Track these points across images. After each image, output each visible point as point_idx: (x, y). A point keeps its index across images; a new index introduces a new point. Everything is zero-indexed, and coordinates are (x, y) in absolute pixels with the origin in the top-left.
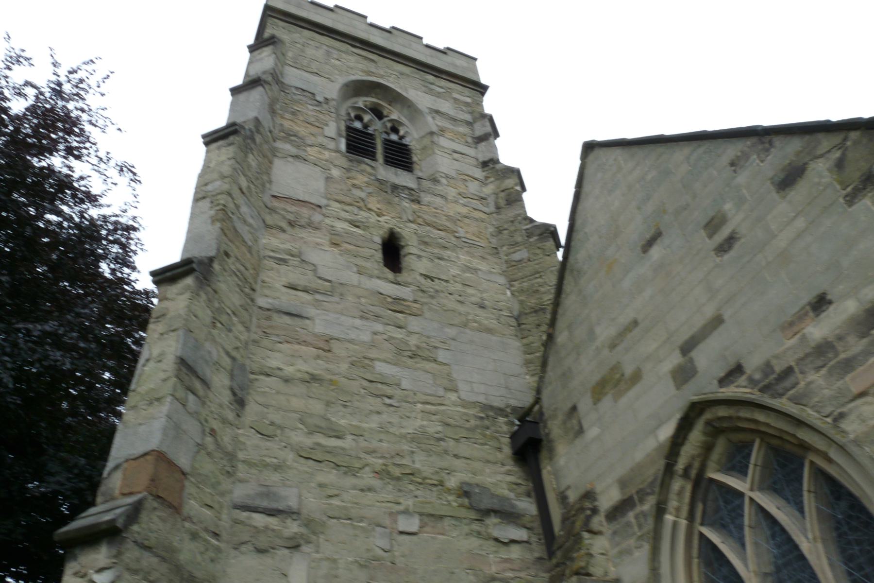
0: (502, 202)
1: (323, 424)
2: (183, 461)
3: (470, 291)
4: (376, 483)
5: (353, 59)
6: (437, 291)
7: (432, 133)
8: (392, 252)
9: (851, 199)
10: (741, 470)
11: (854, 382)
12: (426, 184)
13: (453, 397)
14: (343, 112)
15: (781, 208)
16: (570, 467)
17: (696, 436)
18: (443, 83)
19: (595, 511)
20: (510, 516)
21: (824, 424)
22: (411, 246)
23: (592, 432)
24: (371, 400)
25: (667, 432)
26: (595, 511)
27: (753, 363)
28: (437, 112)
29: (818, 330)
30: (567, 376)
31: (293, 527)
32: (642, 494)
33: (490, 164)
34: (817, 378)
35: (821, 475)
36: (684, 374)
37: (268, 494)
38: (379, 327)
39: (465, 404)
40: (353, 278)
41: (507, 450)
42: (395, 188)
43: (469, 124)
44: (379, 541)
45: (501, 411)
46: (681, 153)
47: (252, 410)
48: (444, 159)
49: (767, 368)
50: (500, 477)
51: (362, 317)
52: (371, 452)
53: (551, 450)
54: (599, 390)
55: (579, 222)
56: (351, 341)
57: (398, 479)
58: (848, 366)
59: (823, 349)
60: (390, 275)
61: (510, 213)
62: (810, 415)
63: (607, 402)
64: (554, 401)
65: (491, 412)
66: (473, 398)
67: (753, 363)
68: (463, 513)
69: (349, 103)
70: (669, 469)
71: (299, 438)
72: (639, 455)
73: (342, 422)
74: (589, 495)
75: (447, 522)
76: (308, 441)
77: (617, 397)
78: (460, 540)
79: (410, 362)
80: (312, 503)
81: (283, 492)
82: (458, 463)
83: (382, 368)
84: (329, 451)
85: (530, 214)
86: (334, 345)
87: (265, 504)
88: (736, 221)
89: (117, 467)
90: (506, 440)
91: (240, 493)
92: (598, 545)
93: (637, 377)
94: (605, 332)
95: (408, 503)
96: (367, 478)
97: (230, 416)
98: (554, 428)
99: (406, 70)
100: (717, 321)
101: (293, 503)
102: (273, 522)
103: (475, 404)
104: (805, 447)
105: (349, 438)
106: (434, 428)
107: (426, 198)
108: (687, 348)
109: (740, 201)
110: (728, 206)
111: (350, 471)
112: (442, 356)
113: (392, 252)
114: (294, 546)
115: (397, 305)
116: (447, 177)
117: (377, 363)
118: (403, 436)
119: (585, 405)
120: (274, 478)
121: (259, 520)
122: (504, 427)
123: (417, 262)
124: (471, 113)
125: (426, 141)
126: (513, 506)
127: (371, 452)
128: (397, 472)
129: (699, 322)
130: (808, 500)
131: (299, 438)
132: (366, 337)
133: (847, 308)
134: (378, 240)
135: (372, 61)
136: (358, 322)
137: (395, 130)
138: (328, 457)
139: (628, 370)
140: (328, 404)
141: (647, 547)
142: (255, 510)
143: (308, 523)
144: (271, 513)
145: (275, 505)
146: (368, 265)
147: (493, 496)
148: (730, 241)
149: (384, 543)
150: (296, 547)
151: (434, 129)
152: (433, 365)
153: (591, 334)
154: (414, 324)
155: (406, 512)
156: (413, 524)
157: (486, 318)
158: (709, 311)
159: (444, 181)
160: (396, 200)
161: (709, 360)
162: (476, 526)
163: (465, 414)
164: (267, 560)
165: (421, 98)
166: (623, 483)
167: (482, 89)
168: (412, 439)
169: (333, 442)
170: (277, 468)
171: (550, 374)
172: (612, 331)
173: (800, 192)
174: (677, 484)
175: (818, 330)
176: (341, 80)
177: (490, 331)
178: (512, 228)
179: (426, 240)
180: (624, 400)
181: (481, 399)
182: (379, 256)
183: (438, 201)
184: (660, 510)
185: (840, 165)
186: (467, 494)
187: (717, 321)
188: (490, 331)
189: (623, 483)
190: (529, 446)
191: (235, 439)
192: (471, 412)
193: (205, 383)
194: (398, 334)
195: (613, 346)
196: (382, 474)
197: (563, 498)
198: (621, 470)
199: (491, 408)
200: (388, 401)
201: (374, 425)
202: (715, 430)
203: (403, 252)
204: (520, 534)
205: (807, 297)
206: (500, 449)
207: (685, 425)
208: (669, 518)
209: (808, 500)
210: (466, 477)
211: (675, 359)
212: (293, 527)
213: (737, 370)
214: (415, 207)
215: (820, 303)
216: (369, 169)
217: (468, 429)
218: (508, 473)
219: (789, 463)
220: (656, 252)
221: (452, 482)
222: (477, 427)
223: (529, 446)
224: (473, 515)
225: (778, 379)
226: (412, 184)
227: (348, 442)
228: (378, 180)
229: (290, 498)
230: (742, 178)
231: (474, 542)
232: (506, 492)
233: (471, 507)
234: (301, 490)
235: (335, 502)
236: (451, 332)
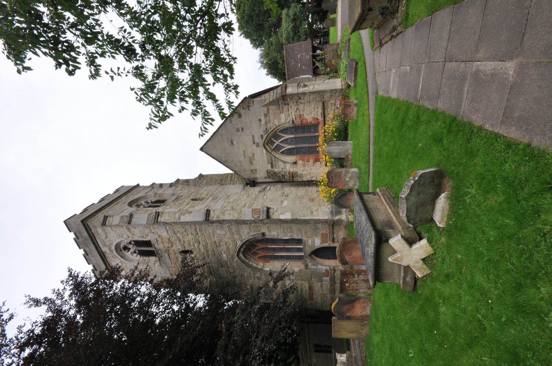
5: (115, 206)
9: (249, 109)
10: (274, 143)
11: (272, 121)
15: (243, 119)
16: (261, 175)
17: (267, 147)
18: (135, 190)
20: (265, 188)
21: (275, 127)
23: (258, 167)
25: (265, 151)
27: (262, 133)
29: (263, 122)
30: (245, 170)
32: (272, 160)
33: (171, 185)
34: (269, 125)
35: (280, 132)
36: (258, 145)
39: (241, 191)
46: (220, 131)
49: (264, 131)
50: (257, 189)
53: (256, 178)
54: (251, 163)
55: (216, 157)
58: (270, 121)
59: (266, 123)
61: (191, 182)
62: (273, 128)
63: (254, 162)
64: (247, 175)
65: (244, 188)
67: (262, 133)
72: (266, 158)
77: (254, 160)
85: (194, 178)
86: (224, 205)
88: (240, 127)
92: (276, 170)
93: (253, 154)
94: (242, 158)
99: (107, 208)
100: (253, 136)
104: (276, 132)
108: (254, 143)
109: (237, 124)
110: (237, 127)
112: (229, 194)
119: (252, 167)
125: (157, 196)
129: (251, 139)
130: (282, 135)
133: (263, 118)
139: (251, 155)
141: (279, 162)
148: (243, 129)
153: (240, 162)
154: (220, 197)
158: (251, 137)
161: (258, 140)
166: (268, 163)
167: (138, 185)
171: (241, 175)
172: (243, 157)
173: (243, 115)
174: (273, 153)
175: (263, 122)
180: (256, 158)
185: (243, 108)
187: (253, 136)
188: (224, 189)
189: (268, 163)
195: (245, 157)
197: (266, 178)
198: (266, 162)
202: (267, 144)
204: (269, 187)
205: (258, 121)
207: (265, 148)
209: (282, 135)
211: (255, 146)
213: (262, 136)
215: (260, 120)
219: (276, 136)
220: (234, 142)
223: (253, 183)
225: (266, 131)
230: (234, 122)
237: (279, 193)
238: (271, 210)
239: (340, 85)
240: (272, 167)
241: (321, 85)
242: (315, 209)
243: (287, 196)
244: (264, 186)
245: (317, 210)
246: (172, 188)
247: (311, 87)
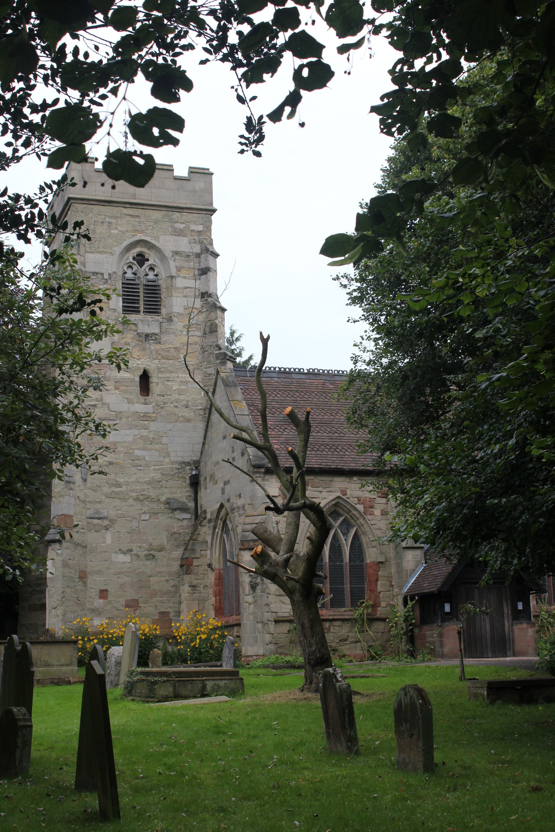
0: (208, 330)
1: (115, 483)
2: (72, 513)
3: (182, 397)
4: (134, 503)
6: (165, 403)
7: (172, 277)
8: (145, 378)
12: (165, 325)
13: (167, 460)
14: (120, 273)
19: (205, 518)
20: (184, 509)
22: (154, 379)
24: (132, 468)
26: (205, 518)
27: (231, 501)
28: (176, 253)
31: (106, 522)
37: (97, 512)
38: (136, 432)
39: (172, 463)
40: (124, 407)
41: (188, 482)
42: (147, 336)
43: (198, 256)
44: (135, 524)
45: (188, 464)
47: (89, 484)
48: (178, 302)
50: (182, 493)
51: (129, 429)
52: (133, 491)
56: (125, 442)
57: (142, 500)
60: (142, 399)
61: (210, 340)
66: (176, 459)
68: (166, 510)
69: (124, 261)
70: (217, 517)
71: (106, 489)
73: (122, 480)
74: (205, 512)
75: (159, 514)
76: (109, 491)
78: (164, 520)
79: (149, 446)
80: (112, 513)
81: (102, 511)
82: (166, 490)
83: (138, 453)
84: (117, 493)
87: (97, 516)
89: (54, 517)
90: (188, 477)
91: (89, 513)
95: (146, 509)
96: (131, 501)
97: (82, 487)
98: (202, 479)
101: (105, 515)
102: (99, 521)
103: (176, 462)
105: (124, 487)
106: (158, 476)
107: (164, 338)
111: (125, 500)
112: (164, 440)
113: (145, 378)
114: (107, 528)
115: (146, 417)
116: (180, 314)
117: (136, 451)
118: (145, 482)
120: (98, 506)
121: (95, 521)
122: (190, 471)
123: (156, 387)
124: (201, 242)
126: (187, 505)
127: (133, 491)
128: (142, 498)
131: (106, 489)
132: (131, 439)
134: (137, 379)
135: (137, 216)
136: (128, 432)
137: (152, 269)
138: (117, 496)
140: (116, 474)
142: (94, 518)
143: (111, 521)
144: (99, 518)
145: (100, 516)
146: (132, 397)
147: (179, 502)
149: (137, 525)
150: (107, 529)
151: (174, 272)
152: (161, 446)
154: (153, 426)
155: (145, 513)
156: (147, 517)
157: (187, 413)
159: (175, 319)
160: (148, 346)
162: (170, 515)
163: (172, 468)
164: (99, 533)
165: (167, 243)
168: (149, 483)
169: (119, 489)
170: (100, 502)
174: (219, 521)
176: (118, 250)
177: (189, 420)
178: (210, 351)
179: (162, 370)
181: (180, 459)
182: (138, 389)
183: (172, 337)
184: (215, 528)
186: (168, 503)
188: (189, 420)
190: (195, 483)
191: (86, 495)
192: (175, 466)
193: (74, 483)
194: (145, 433)
196: (137, 499)
199: (184, 463)
200: (139, 468)
201: (134, 480)
203: (151, 379)
204: (188, 516)
206: (185, 482)
208: (217, 530)
210: (169, 496)
212: (106, 522)
214: (158, 347)
216: (134, 327)
217: (172, 475)
218: (187, 491)
221: (163, 499)
222: (176, 473)
223: (195, 483)
224: (169, 511)
226: (157, 331)
227: (124, 488)
228: (138, 334)
229: (105, 513)
231: (170, 520)
232: (185, 500)
233: (169, 508)
234: (109, 509)
235: (120, 512)
236: (170, 426)
237: (163, 539)
238: (57, 546)
239: (249, 653)
240: (210, 521)
241: (251, 617)
242: (59, 612)
243: (151, 557)
244: (192, 505)
245: (58, 616)
246: (198, 303)
247: (250, 599)
